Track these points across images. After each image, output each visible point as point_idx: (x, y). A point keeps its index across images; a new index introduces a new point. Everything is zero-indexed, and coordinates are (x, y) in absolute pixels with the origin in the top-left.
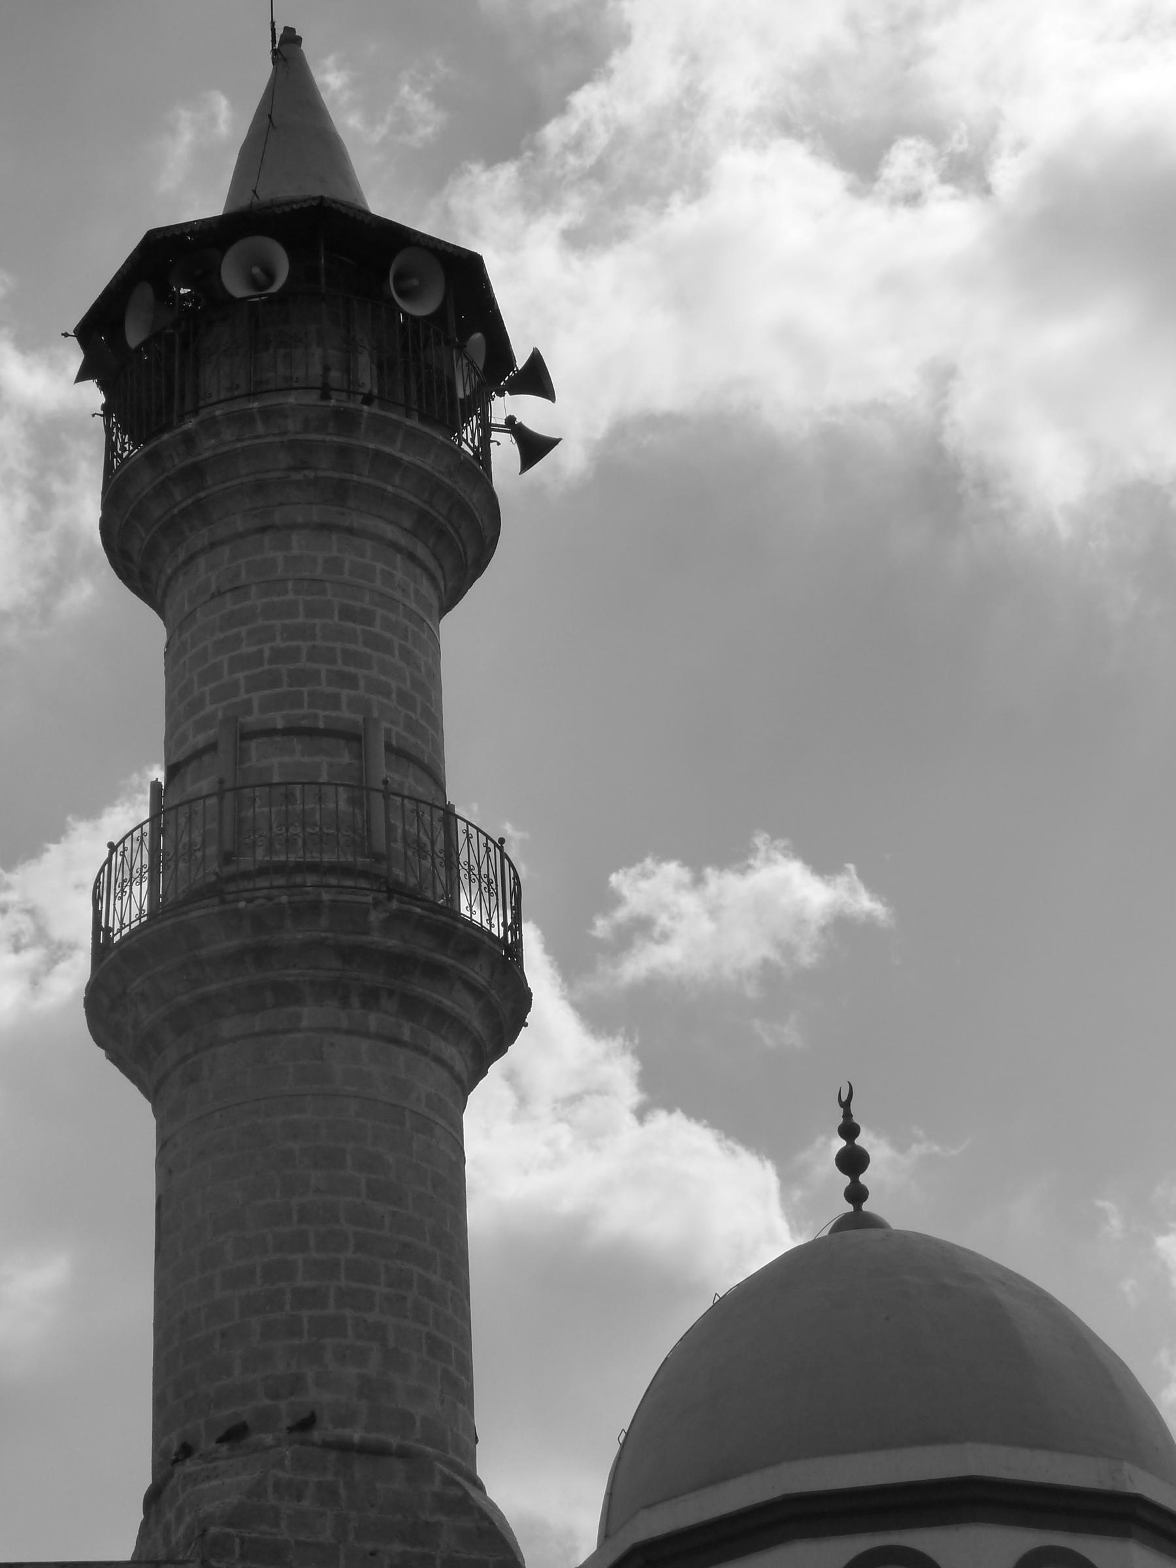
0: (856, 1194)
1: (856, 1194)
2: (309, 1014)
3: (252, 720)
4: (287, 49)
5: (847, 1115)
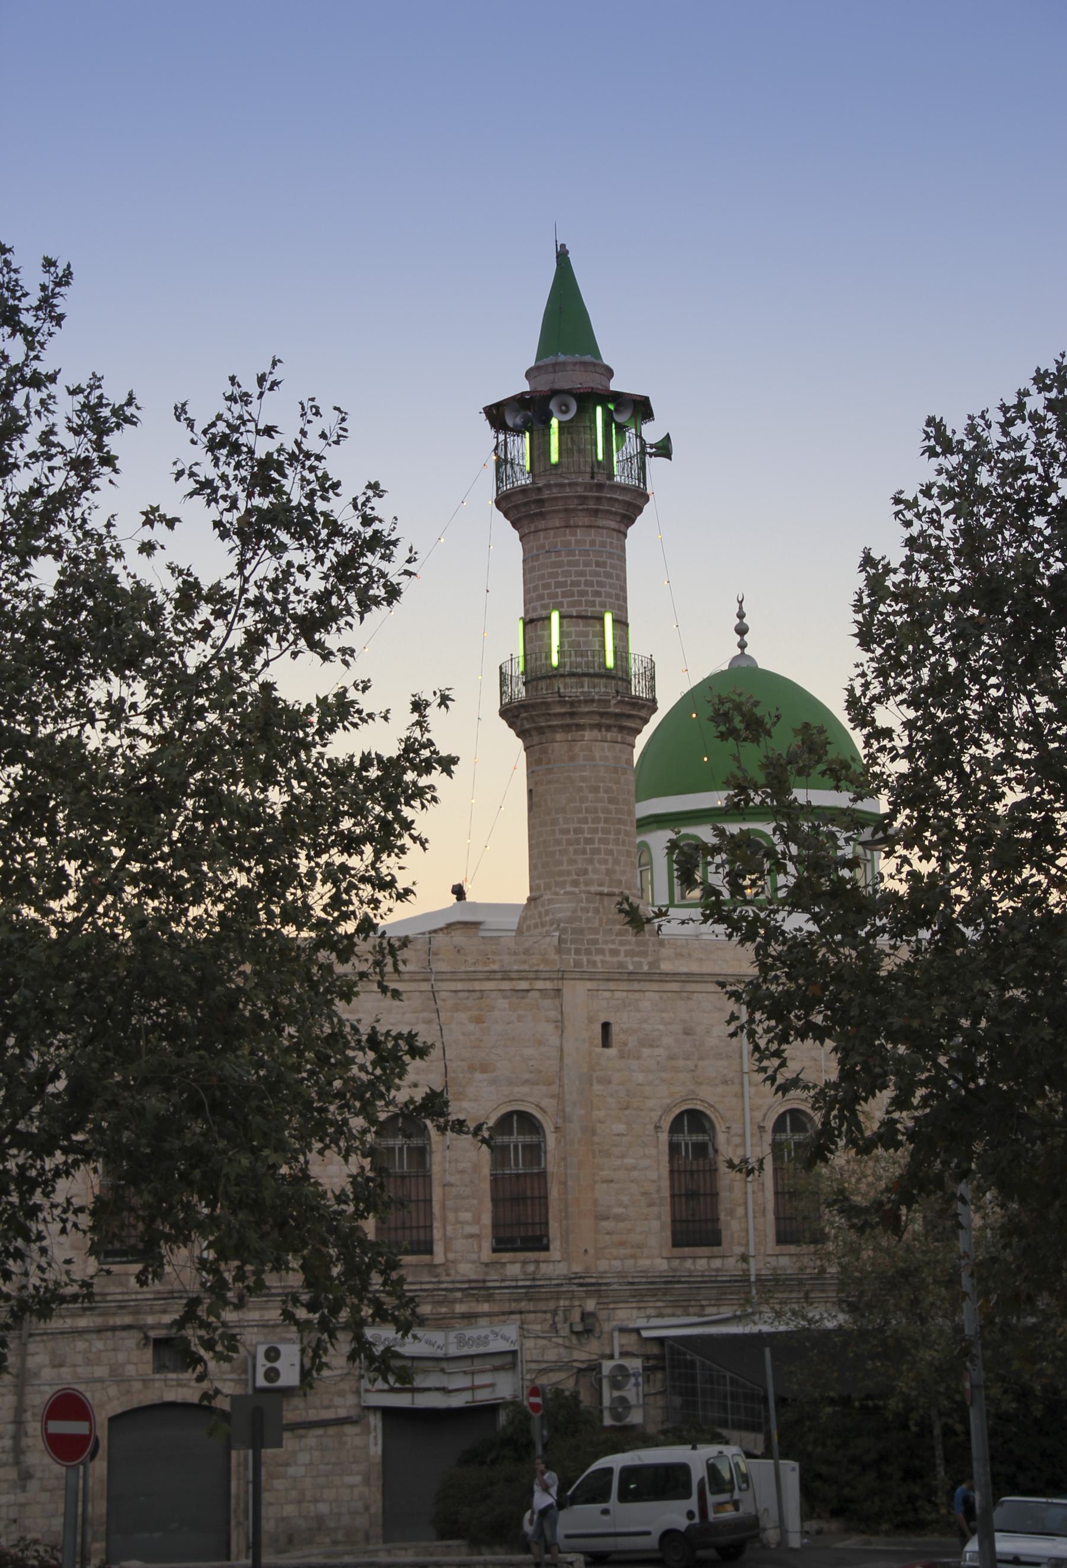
0: (742, 646)
1: (742, 646)
2: (588, 734)
4: (562, 256)
5: (741, 608)
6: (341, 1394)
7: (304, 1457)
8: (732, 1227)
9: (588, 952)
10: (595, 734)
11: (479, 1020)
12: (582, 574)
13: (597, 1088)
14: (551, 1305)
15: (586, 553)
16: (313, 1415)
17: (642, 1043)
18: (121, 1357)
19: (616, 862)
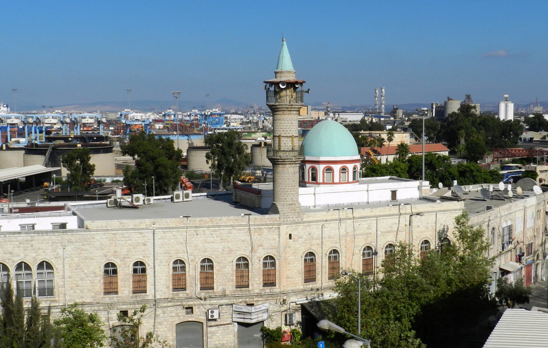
2: (287, 166)
3: (282, 135)
6: (228, 318)
7: (220, 332)
8: (318, 277)
9: (286, 218)
10: (289, 165)
11: (260, 235)
12: (287, 126)
13: (288, 249)
14: (276, 298)
15: (288, 121)
16: (222, 323)
17: (299, 238)
18: (178, 311)
19: (294, 196)
